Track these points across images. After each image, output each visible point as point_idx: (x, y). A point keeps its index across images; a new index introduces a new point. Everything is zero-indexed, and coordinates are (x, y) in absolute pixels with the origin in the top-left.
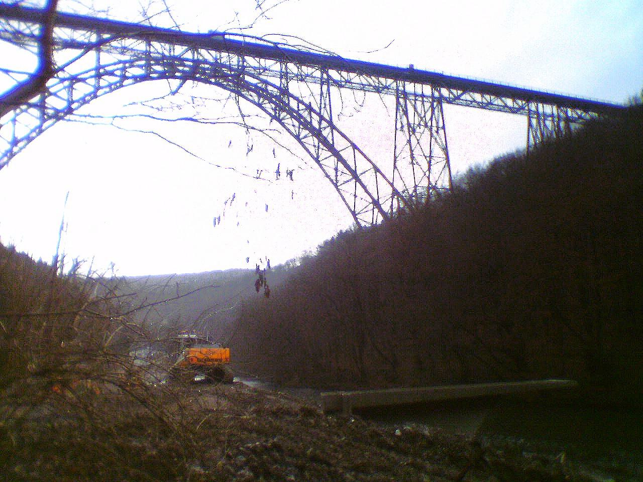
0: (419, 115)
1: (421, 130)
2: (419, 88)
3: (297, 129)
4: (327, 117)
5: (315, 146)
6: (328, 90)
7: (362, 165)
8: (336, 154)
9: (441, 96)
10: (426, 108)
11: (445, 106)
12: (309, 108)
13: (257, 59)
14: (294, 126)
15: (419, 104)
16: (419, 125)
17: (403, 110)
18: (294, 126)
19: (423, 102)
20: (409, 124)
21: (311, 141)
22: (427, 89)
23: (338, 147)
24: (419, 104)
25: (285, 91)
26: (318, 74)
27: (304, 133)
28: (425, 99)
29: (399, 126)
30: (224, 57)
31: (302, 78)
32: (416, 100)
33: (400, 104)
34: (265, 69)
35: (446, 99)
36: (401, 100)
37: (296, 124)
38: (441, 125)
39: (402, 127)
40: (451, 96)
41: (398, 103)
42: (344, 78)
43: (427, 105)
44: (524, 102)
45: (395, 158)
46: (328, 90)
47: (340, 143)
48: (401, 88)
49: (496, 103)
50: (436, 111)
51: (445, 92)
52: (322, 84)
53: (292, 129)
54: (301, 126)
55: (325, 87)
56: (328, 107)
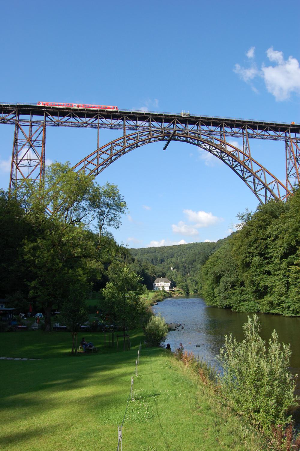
3: (231, 162)
4: (247, 154)
5: (241, 170)
7: (269, 179)
8: (253, 175)
12: (236, 150)
14: (229, 160)
18: (229, 160)
23: (254, 170)
29: (288, 157)
30: (190, 127)
31: (233, 135)
33: (288, 145)
34: (212, 131)
37: (231, 159)
41: (287, 145)
45: (288, 175)
47: (255, 168)
52: (243, 137)
53: (228, 162)
54: (234, 160)
55: (245, 139)
56: (248, 149)
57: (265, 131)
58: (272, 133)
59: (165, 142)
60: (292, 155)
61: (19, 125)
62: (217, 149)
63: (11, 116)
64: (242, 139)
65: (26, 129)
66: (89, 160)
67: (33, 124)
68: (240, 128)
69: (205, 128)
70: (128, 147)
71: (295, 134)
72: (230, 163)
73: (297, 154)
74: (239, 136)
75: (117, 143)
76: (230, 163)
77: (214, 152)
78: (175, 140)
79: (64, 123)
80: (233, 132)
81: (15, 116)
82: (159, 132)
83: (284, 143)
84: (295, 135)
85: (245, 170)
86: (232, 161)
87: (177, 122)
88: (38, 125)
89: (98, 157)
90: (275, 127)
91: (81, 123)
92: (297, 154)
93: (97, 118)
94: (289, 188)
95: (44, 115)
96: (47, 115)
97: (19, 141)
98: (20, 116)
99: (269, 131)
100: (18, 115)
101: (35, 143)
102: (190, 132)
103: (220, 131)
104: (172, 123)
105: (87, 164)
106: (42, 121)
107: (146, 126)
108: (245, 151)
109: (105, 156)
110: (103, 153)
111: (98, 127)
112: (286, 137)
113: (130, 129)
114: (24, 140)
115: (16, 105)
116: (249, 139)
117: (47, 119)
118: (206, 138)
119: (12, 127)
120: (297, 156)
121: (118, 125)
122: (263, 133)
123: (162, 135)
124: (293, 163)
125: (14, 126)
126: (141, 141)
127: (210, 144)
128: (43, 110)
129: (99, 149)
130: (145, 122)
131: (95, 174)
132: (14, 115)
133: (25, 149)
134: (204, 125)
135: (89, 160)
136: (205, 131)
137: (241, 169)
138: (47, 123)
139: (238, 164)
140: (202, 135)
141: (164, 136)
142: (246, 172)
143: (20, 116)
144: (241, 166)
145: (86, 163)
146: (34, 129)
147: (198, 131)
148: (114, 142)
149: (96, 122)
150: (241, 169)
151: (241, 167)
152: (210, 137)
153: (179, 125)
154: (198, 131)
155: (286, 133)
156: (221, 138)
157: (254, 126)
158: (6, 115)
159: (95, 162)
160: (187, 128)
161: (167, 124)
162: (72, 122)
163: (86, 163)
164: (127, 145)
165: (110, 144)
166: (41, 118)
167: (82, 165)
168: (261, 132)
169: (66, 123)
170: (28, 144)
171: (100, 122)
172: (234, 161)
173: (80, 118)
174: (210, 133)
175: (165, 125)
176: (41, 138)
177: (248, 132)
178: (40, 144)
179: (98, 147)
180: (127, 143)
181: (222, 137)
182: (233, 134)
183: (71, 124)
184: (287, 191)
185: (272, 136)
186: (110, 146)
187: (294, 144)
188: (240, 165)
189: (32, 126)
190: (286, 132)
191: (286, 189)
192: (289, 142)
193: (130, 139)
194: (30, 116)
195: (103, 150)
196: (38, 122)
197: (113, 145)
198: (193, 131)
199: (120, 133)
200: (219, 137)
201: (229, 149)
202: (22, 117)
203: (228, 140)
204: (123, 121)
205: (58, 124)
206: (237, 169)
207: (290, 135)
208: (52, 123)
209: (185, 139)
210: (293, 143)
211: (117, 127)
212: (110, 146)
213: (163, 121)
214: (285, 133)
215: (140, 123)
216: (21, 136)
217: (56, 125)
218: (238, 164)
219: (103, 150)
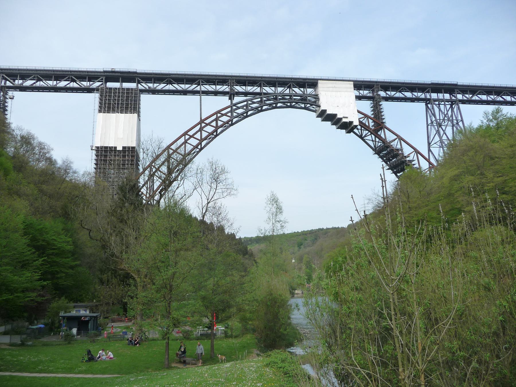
1: (446, 123)
2: (441, 96)
3: (360, 131)
5: (373, 141)
11: (461, 106)
15: (442, 107)
16: (444, 120)
19: (445, 105)
20: (436, 120)
21: (369, 138)
22: (447, 96)
24: (442, 107)
27: (365, 132)
29: (429, 122)
32: (439, 104)
33: (429, 108)
36: (429, 105)
38: (460, 118)
39: (432, 122)
41: (427, 107)
45: (429, 144)
51: (460, 97)
54: (363, 129)
57: (400, 92)
60: (434, 119)
63: (97, 84)
66: (191, 133)
70: (236, 117)
71: (436, 94)
72: (359, 133)
73: (440, 118)
75: (223, 112)
76: (359, 133)
81: (102, 84)
82: (272, 98)
85: (377, 140)
86: (361, 130)
87: (293, 85)
89: (201, 130)
90: (412, 87)
92: (440, 118)
93: (199, 85)
94: (432, 160)
96: (139, 82)
102: (309, 97)
104: (288, 87)
105: (189, 139)
109: (210, 129)
110: (207, 125)
115: (102, 70)
120: (440, 120)
124: (435, 129)
126: (252, 110)
129: (202, 121)
130: (256, 88)
131: (198, 150)
132: (101, 83)
135: (191, 133)
137: (372, 138)
139: (368, 133)
142: (379, 142)
144: (372, 135)
145: (187, 137)
148: (219, 112)
150: (372, 138)
151: (372, 137)
153: (296, 90)
155: (426, 93)
158: (91, 83)
159: (198, 136)
163: (187, 137)
164: (235, 114)
165: (216, 113)
167: (182, 140)
168: (395, 94)
172: (364, 130)
179: (201, 118)
180: (250, 107)
184: (430, 163)
186: (215, 117)
188: (371, 134)
191: (428, 160)
193: (239, 108)
195: (207, 121)
197: (219, 115)
205: (154, 92)
206: (367, 139)
207: (430, 96)
209: (303, 106)
212: (215, 117)
215: (250, 89)
218: (368, 133)
219: (207, 121)
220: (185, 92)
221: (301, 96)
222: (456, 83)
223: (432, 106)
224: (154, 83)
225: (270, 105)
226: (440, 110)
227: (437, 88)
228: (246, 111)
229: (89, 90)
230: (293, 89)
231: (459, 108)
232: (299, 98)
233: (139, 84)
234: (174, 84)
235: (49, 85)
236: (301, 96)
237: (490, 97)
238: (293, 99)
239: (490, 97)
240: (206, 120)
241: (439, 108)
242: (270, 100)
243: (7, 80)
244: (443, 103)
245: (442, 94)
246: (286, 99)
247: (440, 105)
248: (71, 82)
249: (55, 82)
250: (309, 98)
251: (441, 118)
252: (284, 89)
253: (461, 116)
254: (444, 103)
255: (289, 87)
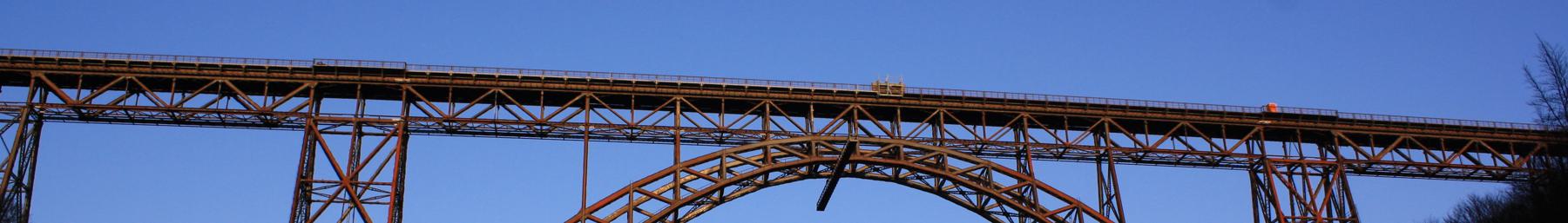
0: (1301, 201)
2: (1293, 149)
6: (1111, 170)
9: (1341, 160)
10: (1314, 188)
11: (1354, 181)
13: (971, 127)
15: (1298, 180)
17: (1267, 194)
19: (1305, 175)
22: (1311, 151)
24: (1298, 180)
25: (1025, 177)
26: (1089, 140)
28: (1309, 170)
30: (907, 128)
31: (1061, 153)
32: (1290, 174)
35: (1349, 163)
36: (1261, 176)
40: (1361, 157)
41: (1255, 181)
42: (1140, 144)
43: (1315, 181)
44: (1516, 157)
46: (1111, 170)
48: (1257, 151)
49: (1456, 161)
50: (1334, 187)
55: (1105, 167)
57: (1176, 135)
58: (1200, 144)
59: (819, 185)
61: (318, 134)
62: (1004, 206)
63: (293, 103)
64: (1094, 165)
65: (339, 145)
67: (365, 129)
68: (1085, 130)
69: (959, 131)
71: (1281, 143)
74: (1083, 158)
77: (995, 213)
78: (854, 174)
79: (470, 125)
80: (1059, 143)
82: (797, 149)
83: (1244, 176)
84: (1284, 147)
88: (381, 132)
90: (1212, 124)
91: (529, 124)
95: (400, 99)
96: (411, 99)
97: (315, 186)
98: (325, 101)
99: (1189, 135)
100: (318, 100)
101: (368, 194)
102: (905, 146)
103: (1014, 140)
106: (394, 119)
107: (750, 131)
108: (1105, 207)
111: (587, 136)
112: (1250, 154)
113: (697, 141)
114: (329, 182)
115: (309, 65)
116: (1118, 167)
117: (414, 111)
118: (962, 166)
119: (293, 140)
120: (1294, 219)
121: (656, 128)
122: (1168, 144)
123: (808, 159)
125: (298, 136)
126: (734, 183)
127: (981, 186)
128: (400, 83)
130: (750, 117)
133: (335, 210)
134: (957, 123)
136: (960, 141)
138: (412, 126)
140: (949, 155)
141: (818, 163)
143: (322, 102)
146: (368, 144)
147: (935, 145)
148: (639, 187)
149: (580, 118)
152: (978, 163)
153: (868, 124)
154: (935, 145)
155: (1251, 141)
156: (1019, 164)
157: (1135, 120)
158: (277, 98)
160: (897, 135)
161: (827, 121)
162: (494, 122)
164: (684, 194)
166: (391, 109)
168: (1161, 141)
169: (475, 125)
170: (343, 195)
171: (594, 118)
173: (524, 106)
174: (979, 148)
175: (820, 124)
176: (388, 175)
177: (1112, 143)
178: (383, 197)
181: (1023, 162)
182: (1061, 150)
183: (493, 125)
185: (1202, 154)
187: (1280, 177)
189: (361, 134)
190: (1250, 138)
192: (1260, 172)
194: (354, 102)
196: (380, 123)
197: (636, 196)
198: (919, 142)
199: (659, 156)
200: (1011, 164)
201: (1047, 202)
202: (377, 108)
203: (1043, 170)
204: (673, 114)
205: (452, 128)
207: (1262, 149)
208: (430, 123)
210: (1274, 175)
211: (655, 136)
213: (812, 110)
214: (1247, 143)
215: (730, 120)
216: (322, 170)
217: (442, 132)
220: (541, 131)
221: (882, 145)
222: (1334, 114)
223: (1268, 179)
224: (454, 101)
225: (790, 169)
226: (1293, 192)
227: (1286, 127)
228: (719, 185)
229: (269, 121)
230: (861, 122)
231: (1346, 188)
232: (877, 149)
233: (412, 106)
234: (512, 103)
235: (161, 105)
236: (882, 145)
237: (1434, 156)
238: (858, 154)
239: (1434, 156)
240: (597, 210)
241: (1289, 187)
242: (791, 155)
243: (48, 89)
244: (1299, 170)
245: (1297, 144)
246: (835, 152)
247: (1294, 176)
248: (221, 98)
249: (178, 97)
250: (906, 150)
251: (1298, 214)
252: (831, 124)
253: (1352, 207)
254: (1303, 169)
255: (849, 118)
